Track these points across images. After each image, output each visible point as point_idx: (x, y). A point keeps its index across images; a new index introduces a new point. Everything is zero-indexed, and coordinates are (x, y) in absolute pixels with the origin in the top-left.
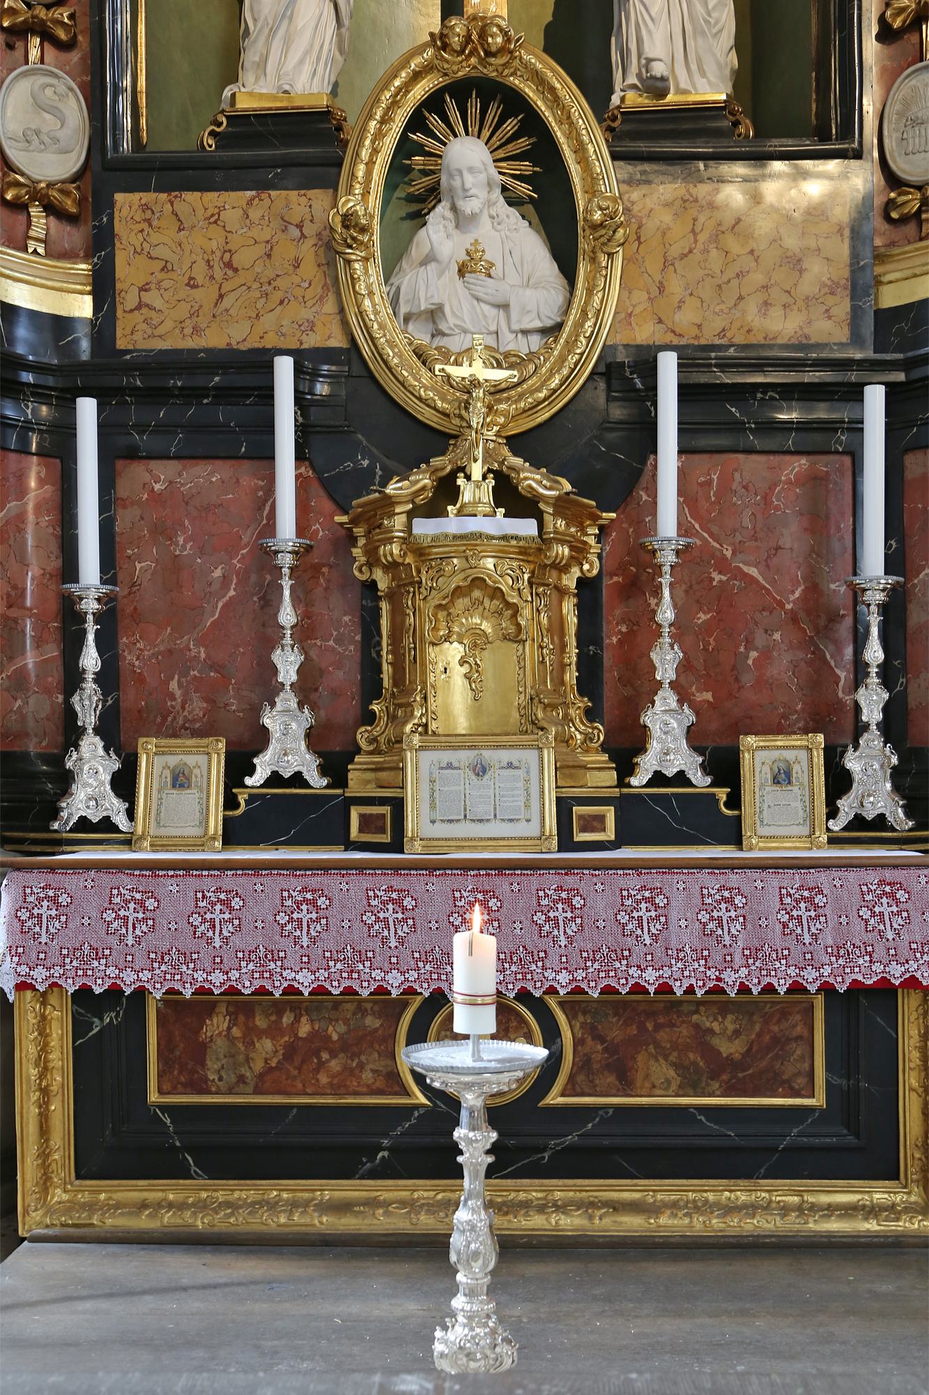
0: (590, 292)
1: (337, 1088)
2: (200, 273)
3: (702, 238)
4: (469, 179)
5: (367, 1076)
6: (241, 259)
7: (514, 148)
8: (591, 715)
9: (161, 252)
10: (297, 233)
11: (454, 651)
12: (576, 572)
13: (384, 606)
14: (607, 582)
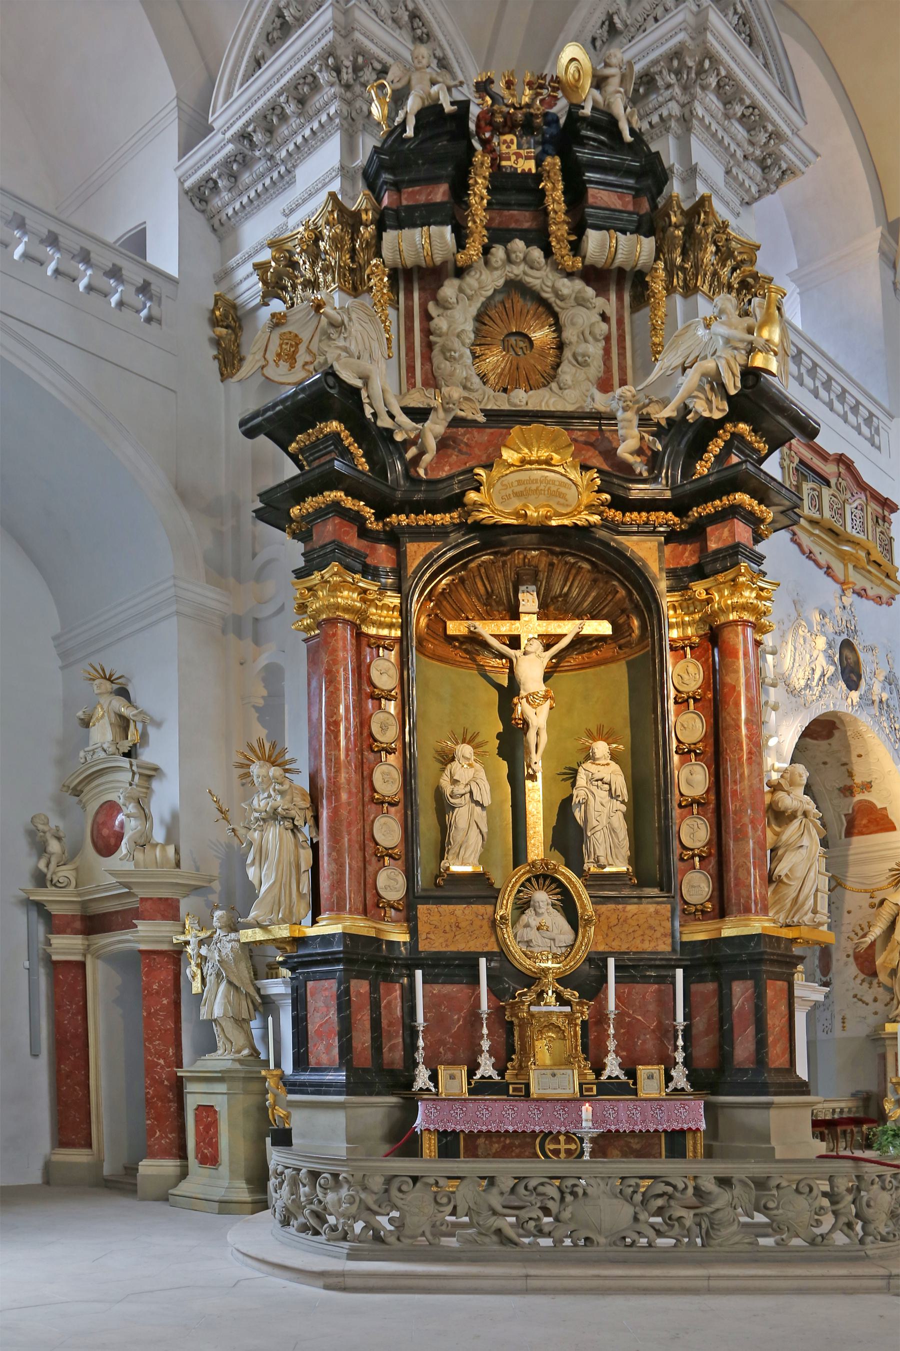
0: (583, 937)
2: (448, 928)
6: (462, 925)
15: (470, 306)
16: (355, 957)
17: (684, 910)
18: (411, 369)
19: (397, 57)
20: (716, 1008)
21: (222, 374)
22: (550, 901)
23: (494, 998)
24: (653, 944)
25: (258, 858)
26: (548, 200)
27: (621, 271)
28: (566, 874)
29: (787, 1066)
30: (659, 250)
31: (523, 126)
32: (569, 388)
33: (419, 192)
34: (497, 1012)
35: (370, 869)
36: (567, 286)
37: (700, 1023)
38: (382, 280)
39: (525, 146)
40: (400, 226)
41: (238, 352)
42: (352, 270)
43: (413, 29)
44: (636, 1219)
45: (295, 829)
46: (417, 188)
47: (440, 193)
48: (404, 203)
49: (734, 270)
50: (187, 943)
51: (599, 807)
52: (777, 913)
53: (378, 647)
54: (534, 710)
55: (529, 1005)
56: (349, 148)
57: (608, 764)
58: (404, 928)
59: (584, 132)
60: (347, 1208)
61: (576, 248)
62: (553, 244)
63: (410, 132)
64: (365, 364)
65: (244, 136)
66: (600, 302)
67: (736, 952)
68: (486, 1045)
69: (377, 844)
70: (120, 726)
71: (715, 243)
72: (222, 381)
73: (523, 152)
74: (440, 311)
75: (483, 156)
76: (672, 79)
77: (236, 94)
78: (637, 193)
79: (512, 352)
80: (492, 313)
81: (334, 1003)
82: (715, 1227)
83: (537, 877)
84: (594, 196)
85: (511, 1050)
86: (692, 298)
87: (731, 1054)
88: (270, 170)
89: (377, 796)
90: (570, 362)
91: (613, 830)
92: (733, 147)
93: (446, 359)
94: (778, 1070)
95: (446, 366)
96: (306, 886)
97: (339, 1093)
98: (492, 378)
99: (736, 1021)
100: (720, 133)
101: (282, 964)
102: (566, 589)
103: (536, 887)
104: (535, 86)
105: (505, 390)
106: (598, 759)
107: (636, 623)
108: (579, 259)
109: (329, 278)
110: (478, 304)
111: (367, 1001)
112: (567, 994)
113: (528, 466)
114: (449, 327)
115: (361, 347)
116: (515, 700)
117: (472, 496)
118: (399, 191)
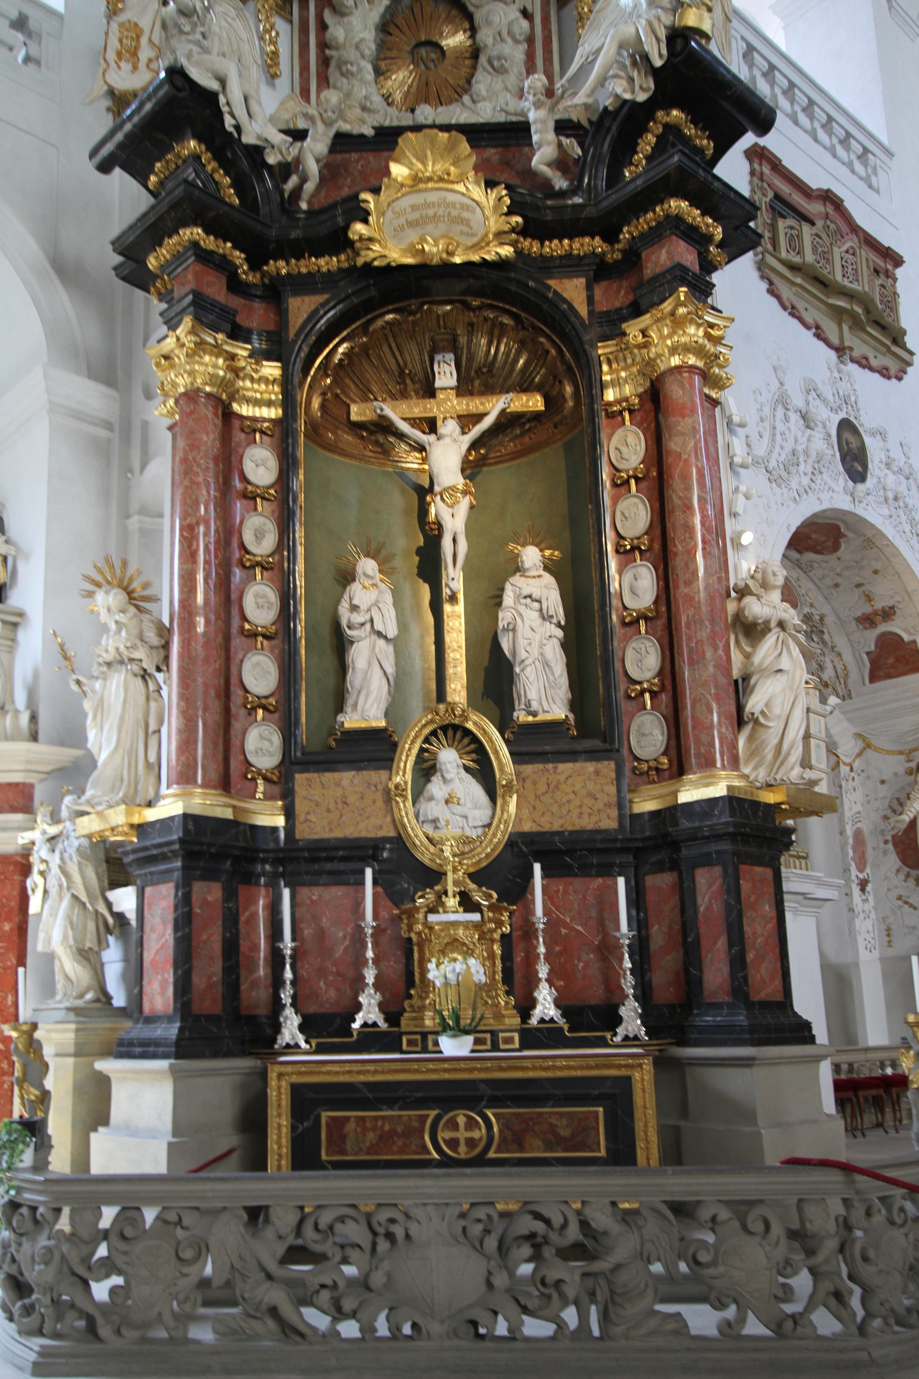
1: (401, 1152)
3: (552, 786)
4: (449, 766)
5: (413, 1147)
7: (468, 749)
8: (508, 993)
10: (373, 788)
12: (499, 931)
13: (416, 948)
14: (515, 934)
15: (371, 10)
20: (678, 911)
22: (460, 762)
24: (594, 819)
32: (484, 99)
35: (236, 726)
37: (658, 935)
51: (529, 633)
52: (755, 768)
54: (450, 510)
57: (539, 576)
69: (246, 691)
79: (423, 67)
80: (399, 20)
83: (444, 728)
89: (247, 626)
90: (485, 69)
91: (546, 664)
93: (343, 75)
99: (703, 929)
103: (445, 743)
106: (528, 570)
107: (568, 389)
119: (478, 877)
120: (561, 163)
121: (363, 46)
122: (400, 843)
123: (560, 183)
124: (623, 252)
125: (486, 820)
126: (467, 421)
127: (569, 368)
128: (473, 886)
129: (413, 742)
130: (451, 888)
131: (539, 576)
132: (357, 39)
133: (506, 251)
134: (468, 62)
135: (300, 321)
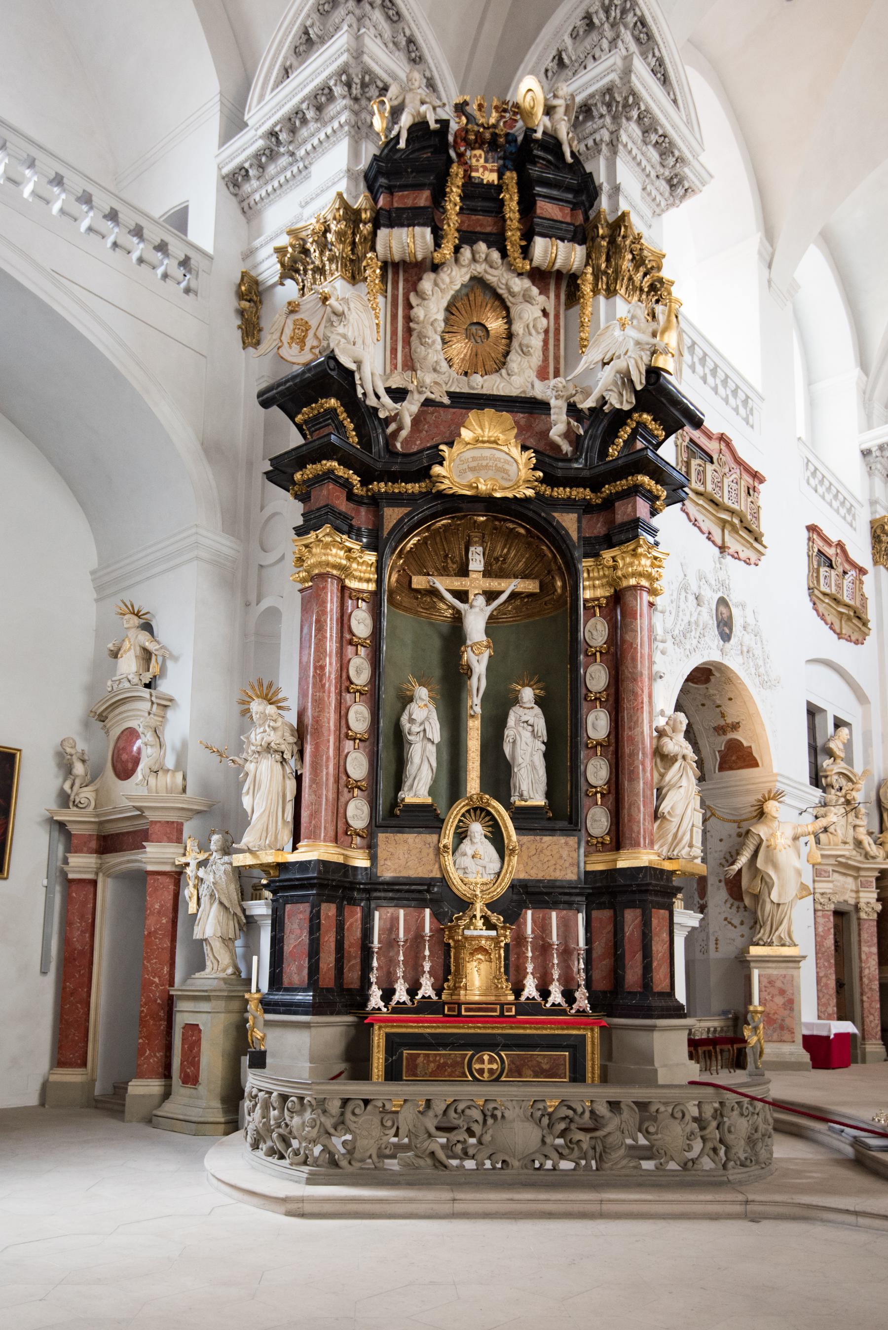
0: (508, 865)
7: (487, 824)
9: (390, 850)
11: (475, 964)
13: (453, 951)
15: (442, 298)
16: (326, 882)
17: (588, 842)
18: (394, 351)
19: (395, 77)
20: (612, 934)
21: (244, 343)
22: (483, 832)
23: (436, 921)
24: (563, 873)
25: (252, 788)
26: (507, 209)
27: (559, 272)
28: (497, 808)
29: (668, 990)
30: (589, 256)
31: (489, 143)
33: (407, 197)
34: (438, 932)
36: (520, 284)
38: (374, 271)
39: (491, 160)
40: (391, 225)
41: (258, 323)
42: (351, 261)
43: (409, 52)
44: (543, 1142)
45: (283, 761)
46: (406, 193)
47: (423, 198)
48: (396, 205)
49: (645, 275)
50: (187, 864)
52: (661, 846)
53: (358, 599)
55: (463, 929)
56: (355, 153)
57: (532, 708)
58: (366, 855)
59: (535, 152)
60: (308, 1132)
61: (526, 252)
62: (508, 247)
63: (402, 144)
64: (359, 351)
65: (273, 134)
66: (542, 298)
67: (628, 882)
68: (427, 966)
70: (143, 659)
71: (631, 252)
72: (244, 349)
73: (489, 166)
74: (419, 301)
75: (458, 168)
76: (604, 110)
77: (267, 98)
78: (575, 206)
79: (473, 340)
80: (459, 305)
81: (306, 925)
82: (607, 1150)
83: (475, 809)
84: (542, 208)
85: (447, 971)
86: (612, 300)
87: (623, 978)
88: (291, 164)
91: (534, 768)
92: (648, 168)
94: (661, 994)
95: (421, 350)
96: (289, 816)
97: (306, 1013)
98: (456, 361)
100: (639, 157)
101: (266, 886)
102: (505, 550)
104: (500, 110)
105: (466, 374)
108: (527, 262)
109: (334, 266)
110: (448, 297)
111: (333, 923)
112: (494, 918)
113: (480, 445)
114: (425, 316)
115: (356, 334)
116: (463, 649)
117: (437, 469)
118: (392, 194)
119: (490, 906)
120: (568, 434)
121: (436, 325)
122: (444, 881)
123: (566, 447)
124: (604, 499)
125: (497, 870)
126: (491, 596)
127: (560, 568)
128: (489, 913)
129: (455, 818)
130: (479, 915)
131: (532, 708)
132: (431, 320)
133: (530, 493)
134: (503, 341)
135: (391, 525)
